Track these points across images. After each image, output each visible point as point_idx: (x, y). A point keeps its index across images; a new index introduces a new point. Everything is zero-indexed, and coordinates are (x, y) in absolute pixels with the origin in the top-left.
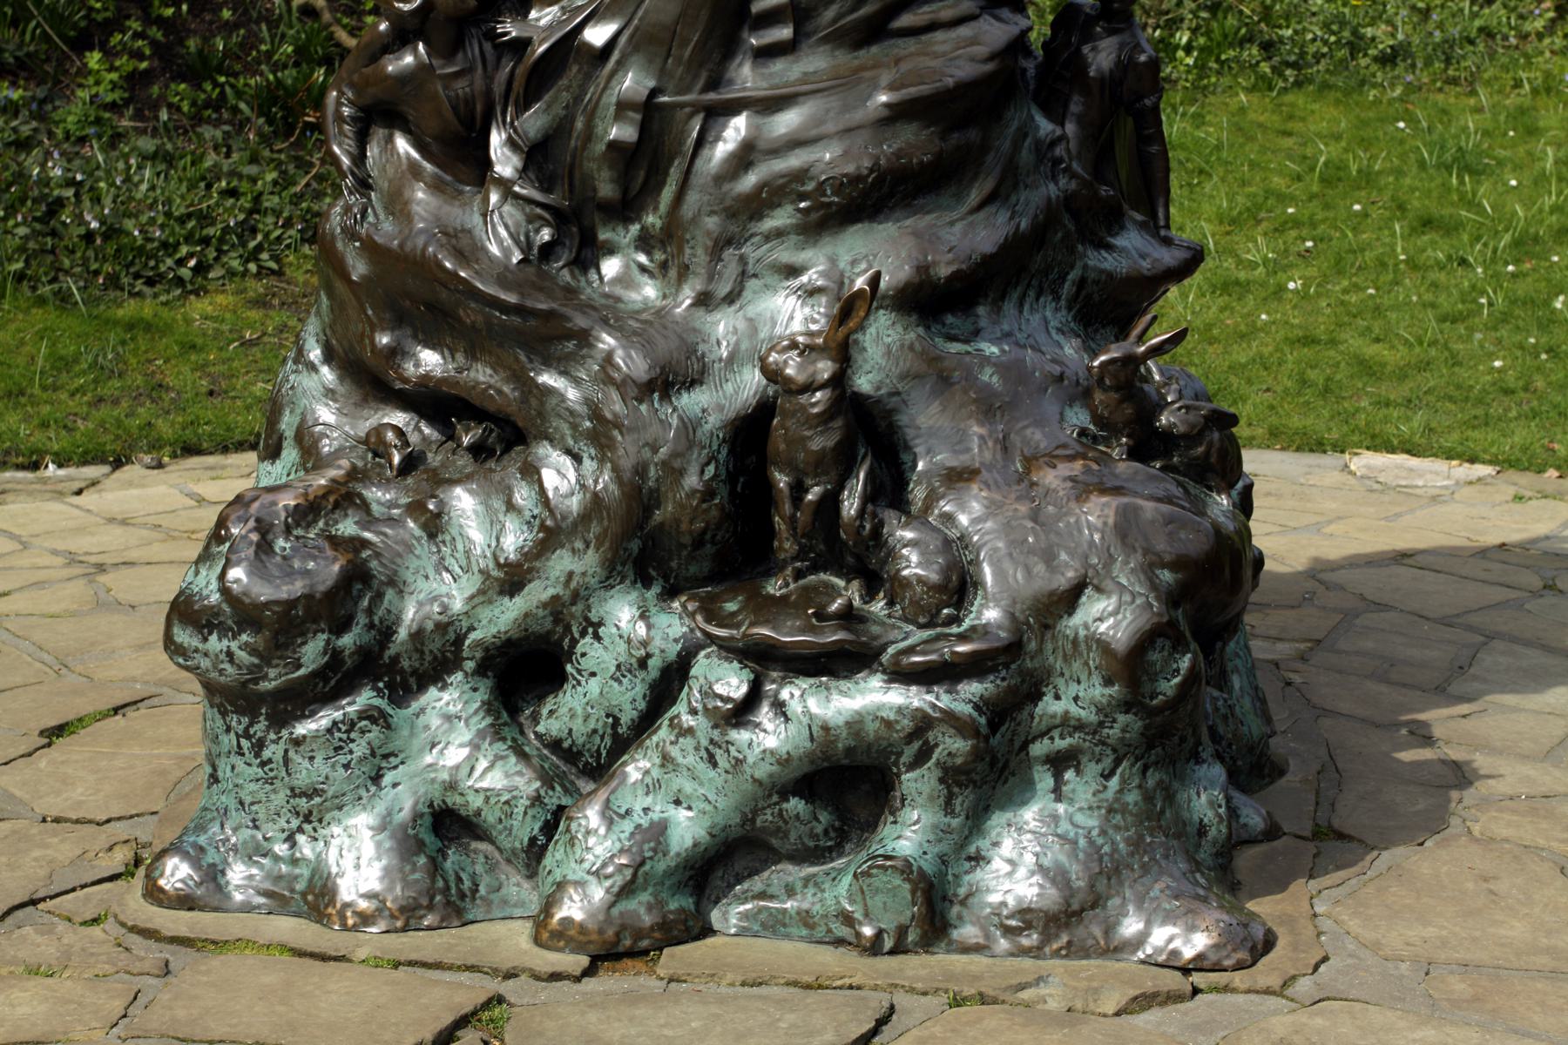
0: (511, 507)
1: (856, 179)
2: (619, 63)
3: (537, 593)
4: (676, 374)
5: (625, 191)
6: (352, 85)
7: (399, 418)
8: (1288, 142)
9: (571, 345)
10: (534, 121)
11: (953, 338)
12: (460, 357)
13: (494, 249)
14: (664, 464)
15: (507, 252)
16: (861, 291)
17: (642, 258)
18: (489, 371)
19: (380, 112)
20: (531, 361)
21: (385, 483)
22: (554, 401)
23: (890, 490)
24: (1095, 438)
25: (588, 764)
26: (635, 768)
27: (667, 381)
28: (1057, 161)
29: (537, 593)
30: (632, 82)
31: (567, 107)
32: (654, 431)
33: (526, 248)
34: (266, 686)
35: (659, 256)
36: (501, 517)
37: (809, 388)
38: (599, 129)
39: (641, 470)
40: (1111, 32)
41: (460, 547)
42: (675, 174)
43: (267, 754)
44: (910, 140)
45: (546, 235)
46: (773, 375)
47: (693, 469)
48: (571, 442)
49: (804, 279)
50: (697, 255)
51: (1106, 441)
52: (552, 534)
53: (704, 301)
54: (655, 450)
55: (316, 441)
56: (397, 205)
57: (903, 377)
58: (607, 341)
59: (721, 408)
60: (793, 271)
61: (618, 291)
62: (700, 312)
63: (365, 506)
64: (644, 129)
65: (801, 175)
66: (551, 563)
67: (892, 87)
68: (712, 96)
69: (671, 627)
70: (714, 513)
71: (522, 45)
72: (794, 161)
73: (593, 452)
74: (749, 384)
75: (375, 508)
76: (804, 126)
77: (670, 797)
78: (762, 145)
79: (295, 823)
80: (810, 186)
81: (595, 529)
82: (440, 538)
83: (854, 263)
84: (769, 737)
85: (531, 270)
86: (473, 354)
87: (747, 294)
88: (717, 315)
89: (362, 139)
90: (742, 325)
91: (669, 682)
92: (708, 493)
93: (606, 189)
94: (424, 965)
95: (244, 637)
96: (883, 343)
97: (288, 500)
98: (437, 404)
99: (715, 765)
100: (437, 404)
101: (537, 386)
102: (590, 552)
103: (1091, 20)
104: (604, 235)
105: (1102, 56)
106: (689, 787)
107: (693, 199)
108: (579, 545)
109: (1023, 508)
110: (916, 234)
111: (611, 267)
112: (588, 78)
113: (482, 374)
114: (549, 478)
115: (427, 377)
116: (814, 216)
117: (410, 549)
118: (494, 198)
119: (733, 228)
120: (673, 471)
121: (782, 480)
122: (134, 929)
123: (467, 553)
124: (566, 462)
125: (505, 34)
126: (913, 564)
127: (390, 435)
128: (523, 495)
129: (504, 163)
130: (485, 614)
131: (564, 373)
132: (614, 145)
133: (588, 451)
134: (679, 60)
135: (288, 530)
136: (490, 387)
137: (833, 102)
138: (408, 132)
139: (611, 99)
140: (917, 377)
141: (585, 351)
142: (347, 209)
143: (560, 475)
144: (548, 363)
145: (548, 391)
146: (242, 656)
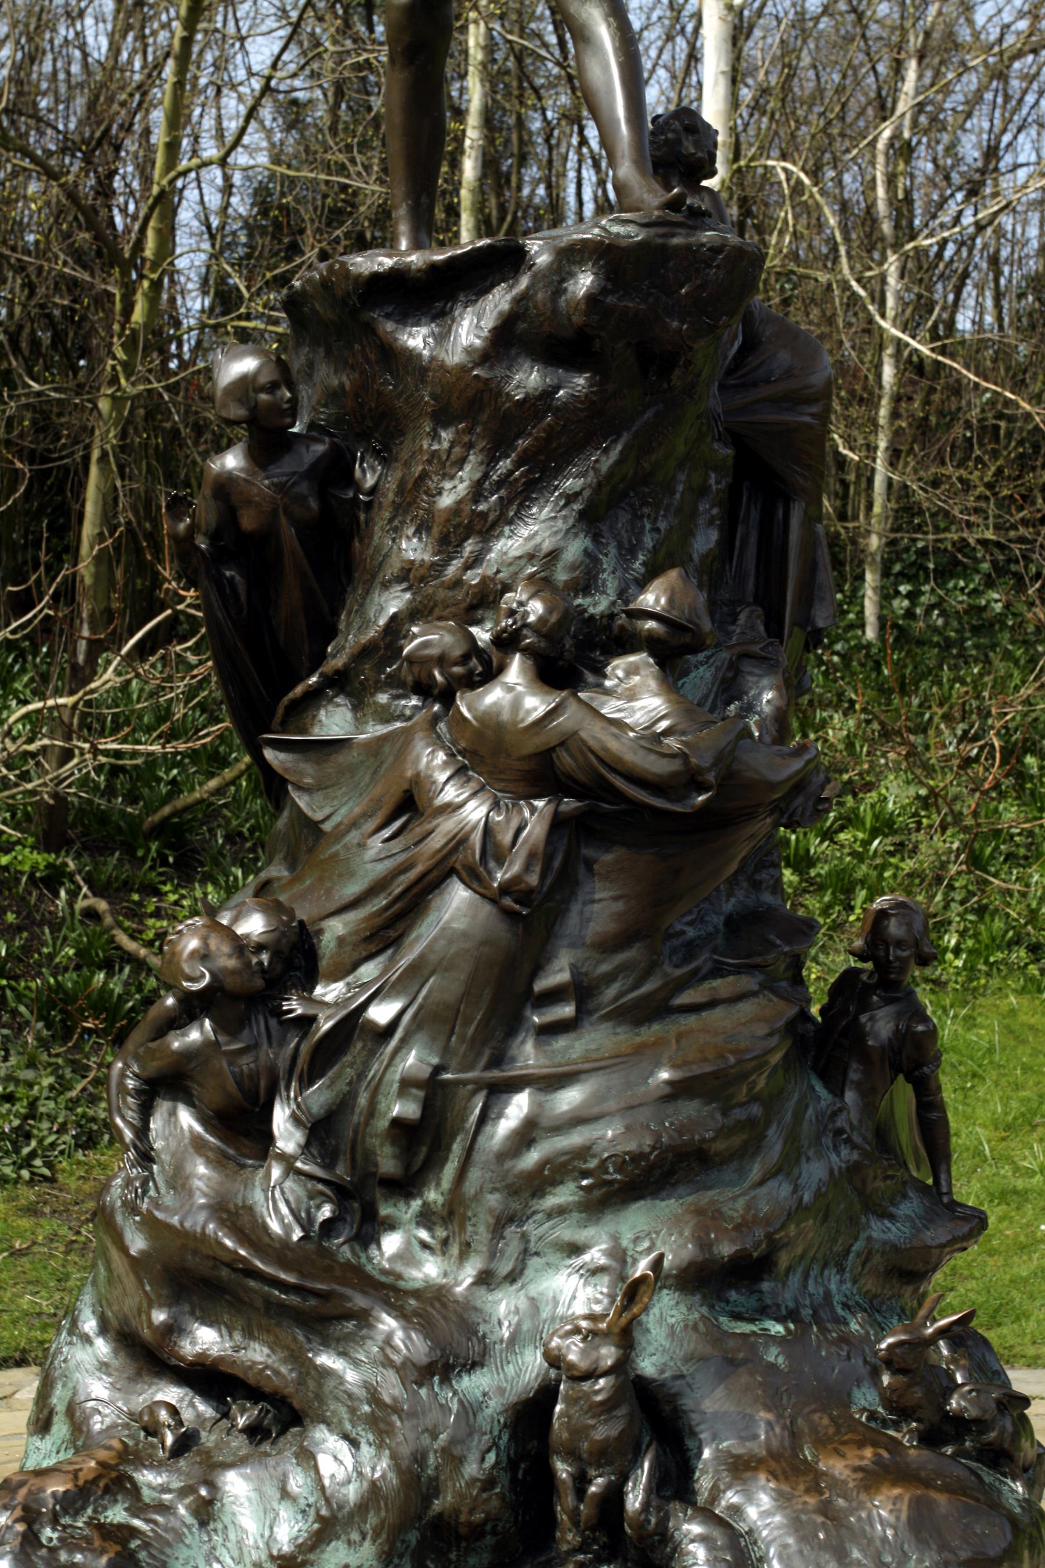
0: (285, 1494)
1: (637, 1157)
2: (404, 1041)
4: (456, 1357)
5: (407, 1167)
6: (137, 1058)
7: (172, 1394)
9: (350, 1325)
10: (319, 1095)
11: (737, 1317)
12: (238, 1336)
13: (275, 1226)
14: (445, 1451)
15: (287, 1229)
16: (644, 1278)
17: (424, 1234)
18: (266, 1351)
19: (167, 1083)
20: (309, 1341)
21: (157, 1466)
22: (331, 1383)
23: (675, 1483)
24: (884, 1423)
27: (444, 1366)
28: (839, 1132)
30: (414, 1060)
31: (350, 1083)
32: (433, 1417)
33: (306, 1224)
35: (441, 1233)
36: (275, 1505)
37: (591, 1375)
38: (382, 1106)
39: (420, 1458)
40: (888, 1001)
41: (232, 1536)
42: (457, 1148)
45: (326, 1212)
46: (554, 1360)
47: (473, 1457)
48: (348, 1426)
49: (586, 1257)
50: (480, 1232)
51: (896, 1425)
52: (328, 1527)
53: (485, 1279)
54: (435, 1437)
55: (87, 1418)
56: (179, 1181)
57: (688, 1359)
58: (388, 1323)
59: (501, 1391)
60: (575, 1249)
61: (399, 1268)
62: (482, 1291)
63: (135, 1491)
64: (427, 1106)
65: (584, 1152)
66: (326, 1556)
67: (674, 1066)
68: (495, 1074)
70: (495, 1503)
71: (307, 1022)
72: (576, 1138)
73: (371, 1437)
74: (529, 1367)
75: (146, 1492)
76: (584, 1105)
78: (545, 1122)
80: (593, 1164)
82: (212, 1526)
83: (636, 1240)
85: (310, 1246)
86: (249, 1334)
87: (529, 1272)
88: (498, 1295)
89: (146, 1111)
90: (523, 1303)
92: (489, 1483)
93: (387, 1163)
96: (666, 1316)
97: (57, 1487)
98: (210, 1379)
100: (210, 1379)
101: (316, 1367)
102: (367, 1543)
103: (868, 989)
104: (385, 1210)
105: (881, 1025)
107: (475, 1175)
108: (355, 1536)
109: (812, 1501)
110: (699, 1212)
111: (391, 1243)
112: (372, 1053)
113: (258, 1354)
114: (326, 1465)
115: (203, 1355)
116: (597, 1193)
117: (180, 1537)
118: (276, 1172)
119: (515, 1205)
120: (453, 1458)
121: (563, 1470)
123: (240, 1543)
124: (343, 1448)
125: (291, 1011)
127: (163, 1415)
128: (298, 1482)
129: (285, 1129)
132: (397, 1123)
133: (366, 1437)
134: (462, 1038)
135: (55, 1522)
136: (267, 1367)
137: (615, 1079)
138: (190, 1104)
139: (396, 1075)
140: (702, 1359)
141: (364, 1332)
142: (128, 1182)
143: (339, 1461)
144: (327, 1343)
145: (326, 1373)
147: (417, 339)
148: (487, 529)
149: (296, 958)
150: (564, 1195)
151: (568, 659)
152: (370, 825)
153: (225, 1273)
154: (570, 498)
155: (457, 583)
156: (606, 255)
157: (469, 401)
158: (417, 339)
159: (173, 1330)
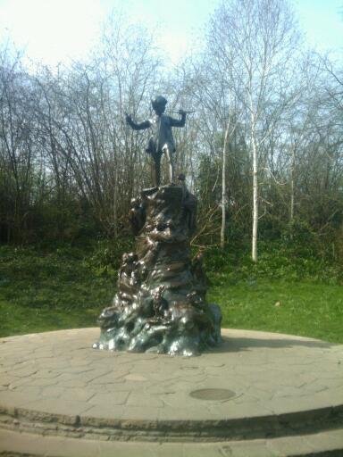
25: (134, 335)
26: (139, 336)
44: (171, 274)
69: (145, 321)
77: (141, 338)
84: (150, 332)
91: (143, 326)
93: (142, 278)
98: (125, 299)
126: (166, 315)
143: (134, 306)
147: (149, 197)
148: (155, 216)
149: (136, 258)
151: (161, 228)
156: (165, 189)
157: (154, 203)
158: (149, 197)
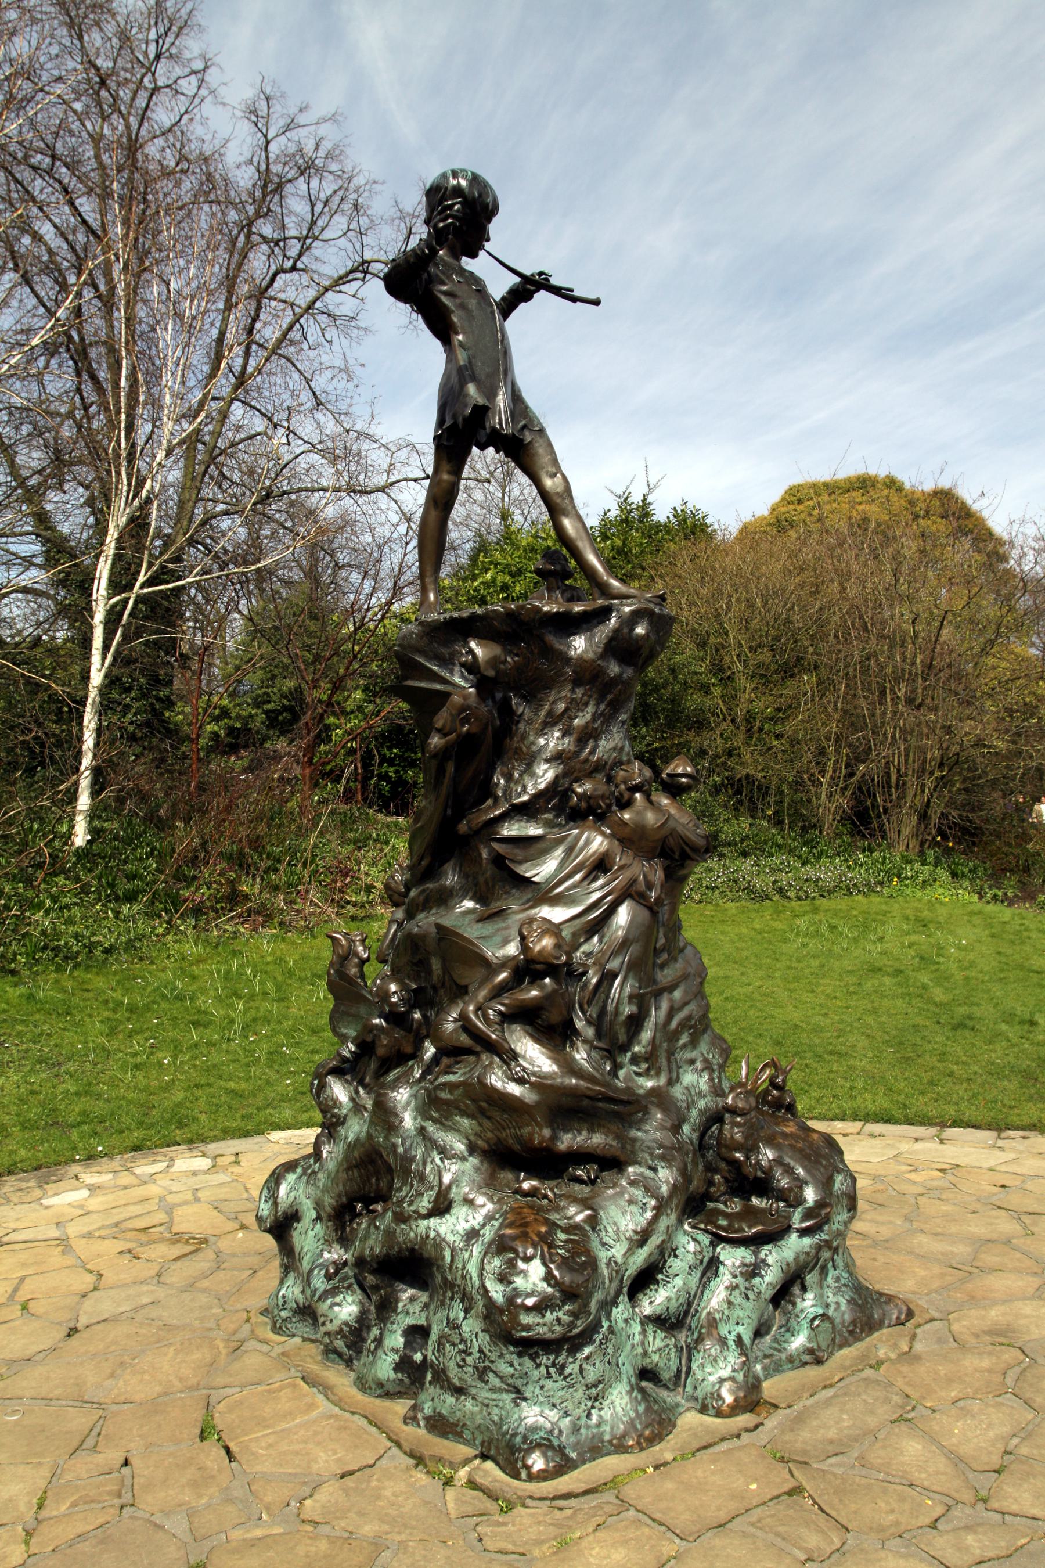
3: (655, 1241)
8: (91, 995)
17: (635, 1068)
22: (638, 1144)
29: (655, 1241)
34: (576, 1331)
43: (567, 1371)
79: (589, 1404)
81: (675, 1201)
86: (592, 1130)
94: (705, 1448)
95: (567, 1307)
99: (748, 1299)
106: (741, 1313)
122: (554, 1498)
130: (631, 1260)
131: (639, 1129)
146: (566, 1319)
150: (684, 1039)
152: (578, 877)
153: (586, 1102)
154: (623, 722)
155: (586, 760)
159: (554, 1138)
